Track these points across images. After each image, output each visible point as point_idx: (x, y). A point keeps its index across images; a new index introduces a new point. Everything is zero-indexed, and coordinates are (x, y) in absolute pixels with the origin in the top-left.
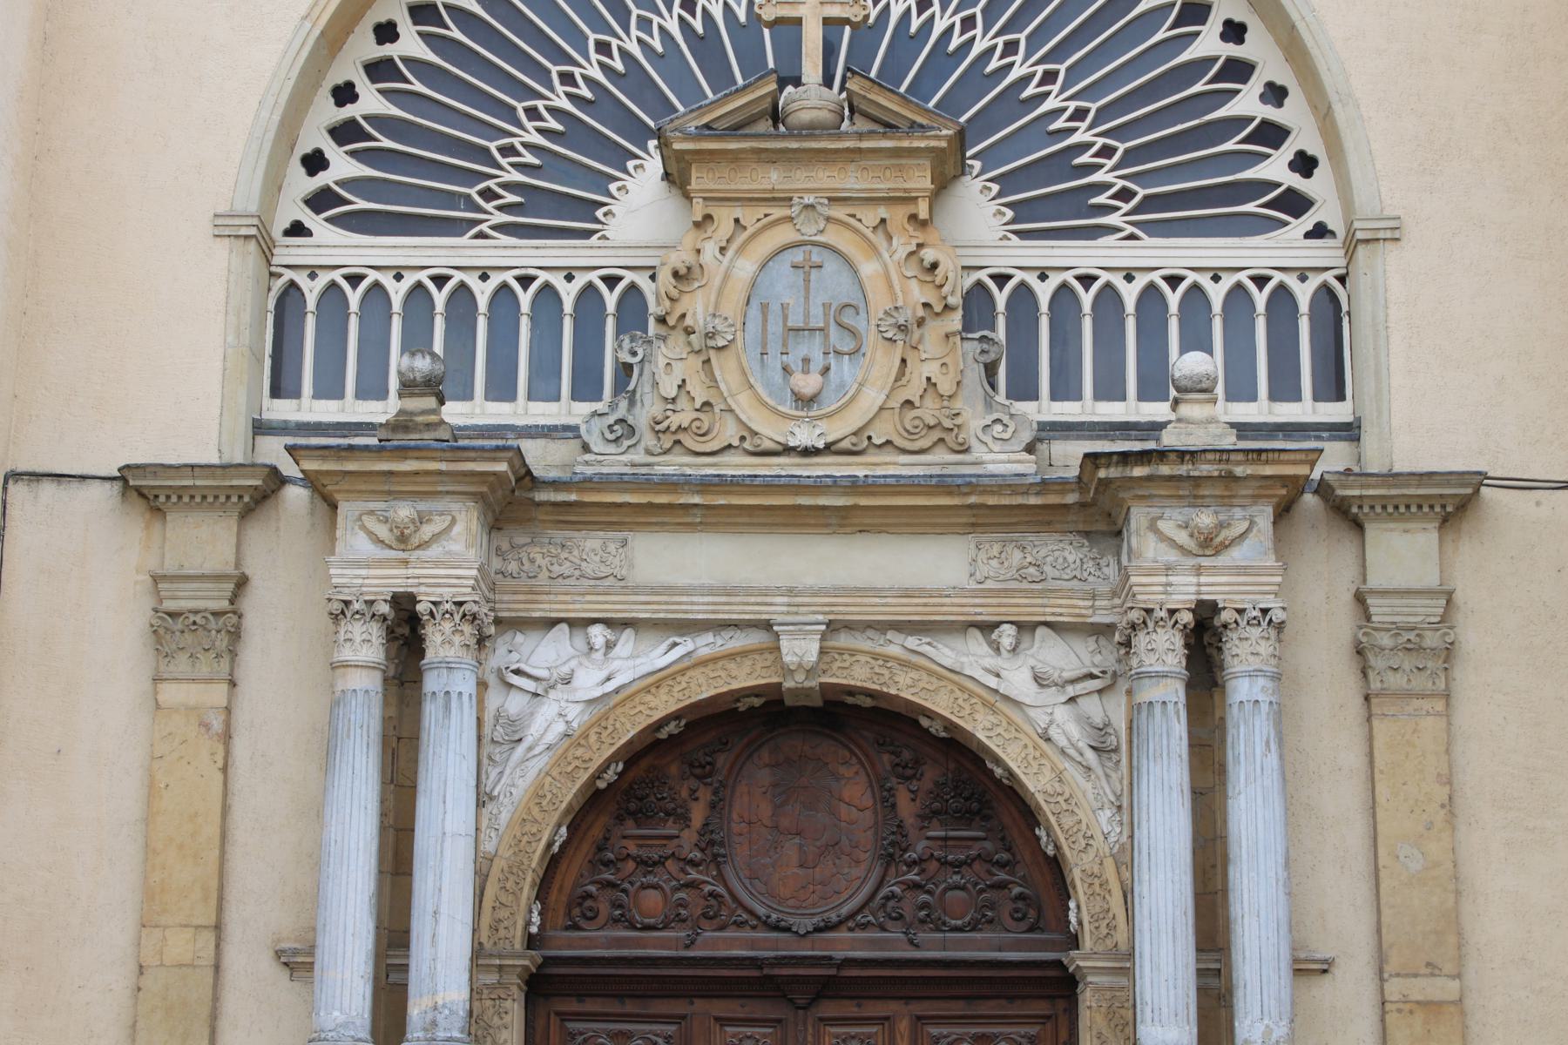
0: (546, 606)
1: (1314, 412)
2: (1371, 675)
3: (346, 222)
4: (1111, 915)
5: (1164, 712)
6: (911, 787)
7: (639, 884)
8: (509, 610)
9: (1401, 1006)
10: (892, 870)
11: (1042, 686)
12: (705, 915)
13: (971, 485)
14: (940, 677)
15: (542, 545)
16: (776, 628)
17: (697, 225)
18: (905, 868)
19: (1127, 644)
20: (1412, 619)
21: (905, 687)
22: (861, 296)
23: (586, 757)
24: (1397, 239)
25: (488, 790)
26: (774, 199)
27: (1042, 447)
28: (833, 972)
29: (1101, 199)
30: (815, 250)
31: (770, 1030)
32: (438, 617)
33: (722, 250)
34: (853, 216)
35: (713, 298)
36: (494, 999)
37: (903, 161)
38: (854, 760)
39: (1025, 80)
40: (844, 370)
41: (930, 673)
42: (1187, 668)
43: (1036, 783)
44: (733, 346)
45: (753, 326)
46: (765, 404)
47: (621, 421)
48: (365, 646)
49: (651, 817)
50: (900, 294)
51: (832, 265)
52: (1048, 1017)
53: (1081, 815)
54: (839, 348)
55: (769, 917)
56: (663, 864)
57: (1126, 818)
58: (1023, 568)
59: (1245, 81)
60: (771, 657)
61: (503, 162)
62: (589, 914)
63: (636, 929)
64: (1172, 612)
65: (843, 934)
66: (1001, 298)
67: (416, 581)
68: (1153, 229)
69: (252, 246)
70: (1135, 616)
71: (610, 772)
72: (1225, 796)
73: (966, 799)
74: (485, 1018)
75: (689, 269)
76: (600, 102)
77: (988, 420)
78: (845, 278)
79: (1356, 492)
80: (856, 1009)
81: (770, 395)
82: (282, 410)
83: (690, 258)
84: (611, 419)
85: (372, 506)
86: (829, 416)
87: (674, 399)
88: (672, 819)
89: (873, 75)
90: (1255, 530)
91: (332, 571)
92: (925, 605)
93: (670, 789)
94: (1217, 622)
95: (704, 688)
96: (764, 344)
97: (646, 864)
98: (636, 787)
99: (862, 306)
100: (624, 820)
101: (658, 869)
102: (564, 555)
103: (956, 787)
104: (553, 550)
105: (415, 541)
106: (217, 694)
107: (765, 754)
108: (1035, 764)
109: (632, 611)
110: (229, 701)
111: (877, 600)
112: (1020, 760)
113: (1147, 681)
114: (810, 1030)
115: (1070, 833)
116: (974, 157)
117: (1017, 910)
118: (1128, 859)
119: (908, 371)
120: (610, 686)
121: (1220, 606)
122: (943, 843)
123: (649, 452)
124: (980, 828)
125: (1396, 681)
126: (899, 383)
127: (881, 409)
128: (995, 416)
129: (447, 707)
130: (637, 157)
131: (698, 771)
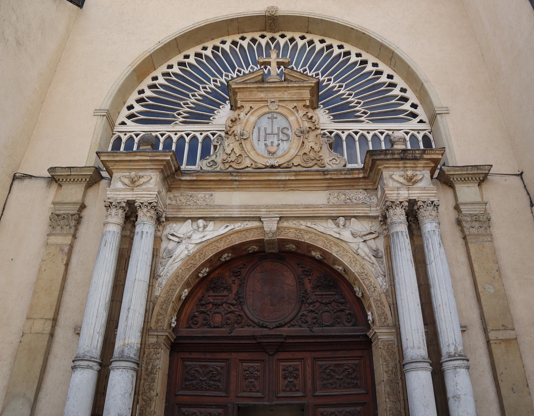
0: (184, 213)
4: (385, 314)
6: (309, 278)
8: (171, 214)
9: (496, 341)
10: (303, 306)
14: (319, 236)
15: (184, 196)
18: (308, 305)
20: (475, 212)
21: (306, 239)
22: (289, 125)
24: (448, 113)
25: (159, 274)
26: (262, 101)
28: (283, 340)
29: (358, 114)
30: (275, 114)
31: (260, 364)
36: (154, 349)
41: (316, 234)
44: (249, 138)
49: (218, 289)
51: (280, 118)
52: (362, 357)
53: (372, 280)
54: (282, 139)
55: (259, 323)
56: (222, 305)
58: (345, 200)
62: (195, 323)
64: (401, 202)
65: (286, 329)
67: (136, 196)
68: (373, 121)
74: (150, 356)
75: (236, 119)
78: (284, 120)
79: (452, 173)
85: (124, 174)
87: (230, 154)
88: (226, 290)
90: (425, 178)
91: (108, 193)
92: (313, 211)
93: (225, 280)
95: (236, 241)
98: (214, 280)
100: (209, 291)
101: (221, 307)
104: (188, 197)
109: (213, 214)
111: (297, 209)
112: (348, 262)
115: (368, 286)
116: (321, 104)
117: (348, 319)
119: (305, 145)
120: (204, 239)
121: (417, 200)
124: (334, 291)
125: (474, 231)
126: (301, 148)
127: (296, 155)
128: (333, 158)
131: (235, 274)
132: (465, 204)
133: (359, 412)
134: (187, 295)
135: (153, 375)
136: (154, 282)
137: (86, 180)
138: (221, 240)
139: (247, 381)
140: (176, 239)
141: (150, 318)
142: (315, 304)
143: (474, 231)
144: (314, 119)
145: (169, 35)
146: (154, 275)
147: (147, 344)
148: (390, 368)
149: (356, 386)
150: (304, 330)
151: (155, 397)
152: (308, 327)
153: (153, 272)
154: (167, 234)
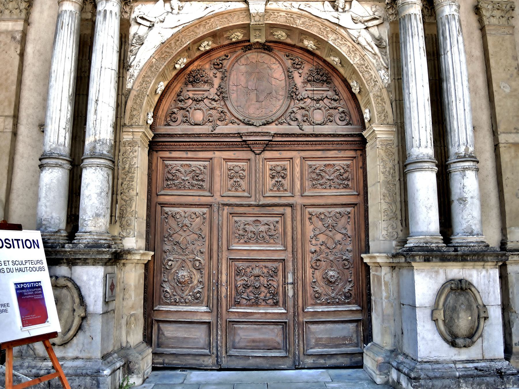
7: (194, 108)
10: (292, 103)
18: (297, 102)
28: (271, 138)
31: (246, 163)
38: (277, 62)
41: (310, 19)
49: (199, 83)
52: (355, 157)
53: (372, 72)
55: (244, 120)
56: (203, 101)
73: (321, 76)
80: (279, 155)
88: (206, 84)
97: (197, 101)
98: (192, 73)
101: (202, 103)
103: (317, 72)
107: (242, 60)
122: (312, 92)
131: (216, 66)
134: (163, 89)
135: (130, 175)
136: (124, 72)
138: (199, 25)
139: (232, 180)
140: (148, 24)
141: (123, 114)
142: (306, 100)
146: (124, 66)
147: (122, 142)
148: (388, 169)
150: (294, 128)
151: (135, 197)
152: (298, 126)
153: (122, 61)
154: (135, 17)
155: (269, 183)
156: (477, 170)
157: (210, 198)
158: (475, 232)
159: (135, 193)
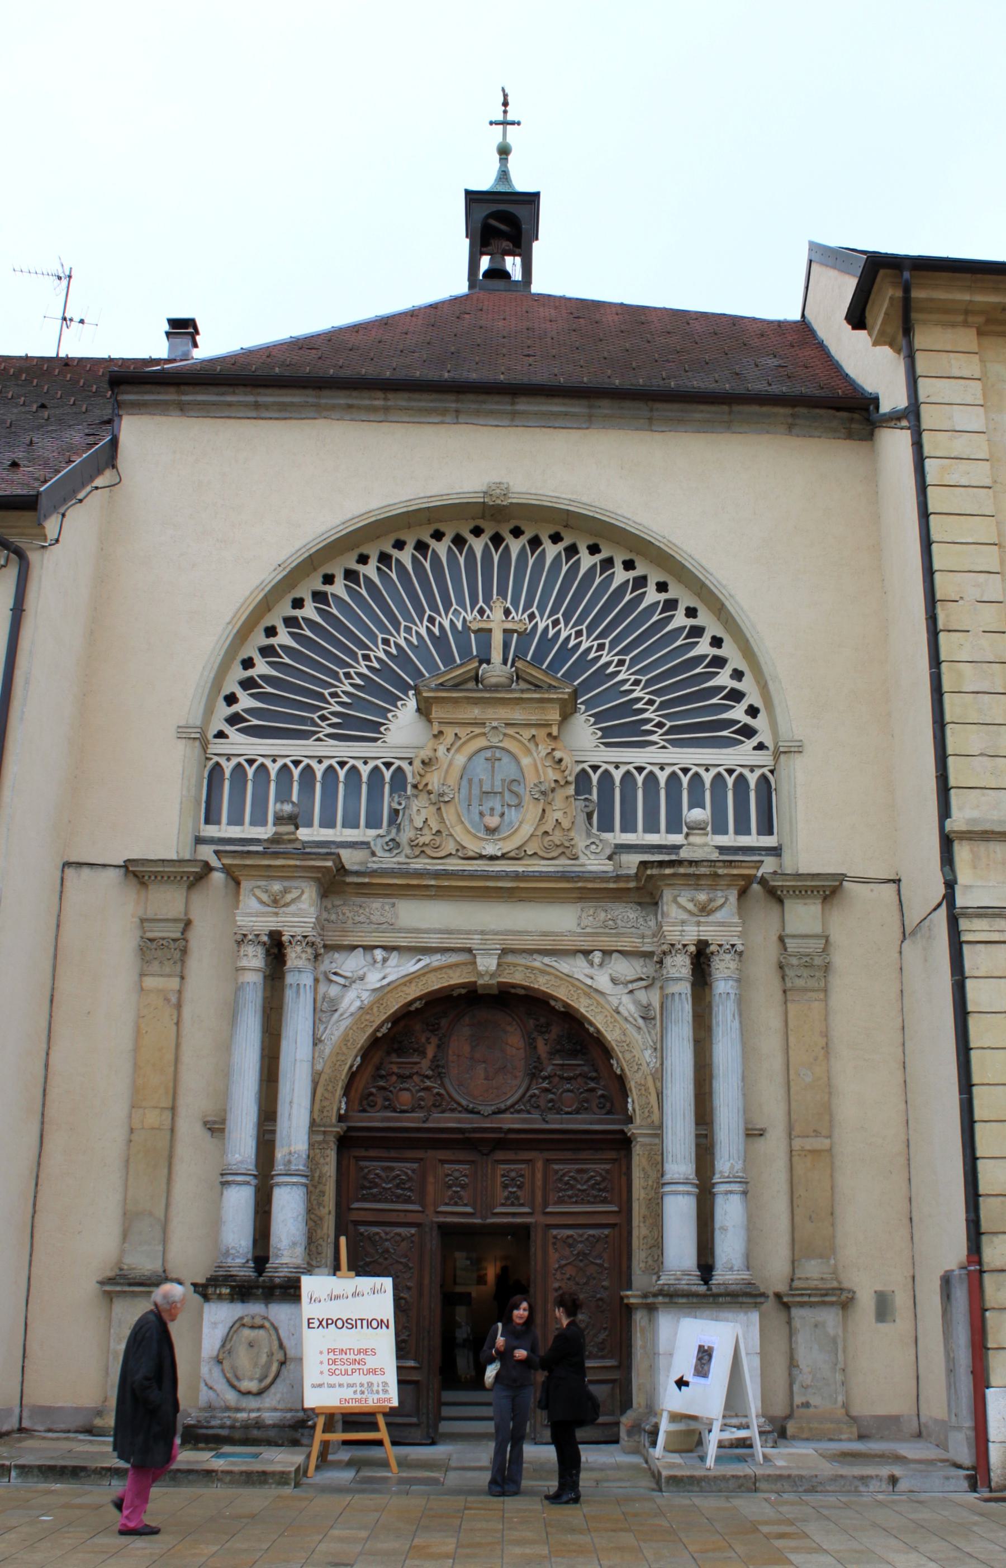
1: (758, 840)
2: (787, 979)
3: (246, 731)
5: (680, 999)
8: (331, 940)
10: (534, 1082)
11: (615, 984)
12: (434, 1105)
13: (579, 877)
14: (561, 979)
16: (474, 952)
17: (435, 736)
18: (541, 1080)
19: (661, 962)
20: (807, 950)
21: (542, 984)
23: (372, 1020)
27: (616, 857)
28: (502, 1135)
29: (648, 727)
30: (498, 751)
32: (294, 943)
33: (448, 750)
34: (518, 733)
35: (443, 775)
37: (545, 705)
38: (514, 1023)
39: (608, 664)
40: (512, 815)
41: (556, 977)
42: (692, 976)
43: (611, 1036)
45: (464, 791)
46: (469, 832)
47: (393, 840)
48: (255, 958)
50: (542, 774)
51: (506, 759)
53: (635, 1053)
54: (510, 803)
57: (659, 1054)
59: (722, 667)
60: (471, 967)
61: (332, 701)
62: (372, 1104)
63: (395, 1111)
64: (685, 946)
65: (508, 1116)
66: (595, 778)
68: (675, 743)
69: (197, 743)
70: (665, 947)
71: (384, 1028)
72: (711, 1044)
73: (574, 1044)
75: (430, 759)
76: (383, 670)
77: (588, 842)
78: (513, 766)
79: (780, 884)
81: (472, 827)
82: (211, 831)
83: (430, 754)
84: (387, 839)
86: (504, 839)
87: (421, 829)
88: (416, 1053)
89: (528, 659)
91: (237, 918)
92: (554, 940)
94: (708, 951)
95: (435, 983)
96: (470, 800)
99: (522, 780)
102: (361, 911)
105: (282, 903)
106: (174, 983)
108: (611, 1026)
110: (181, 987)
111: (528, 937)
113: (671, 982)
114: (490, 1166)
116: (581, 703)
118: (660, 1077)
119: (546, 815)
123: (407, 857)
125: (800, 983)
127: (532, 835)
129: (298, 992)
130: (403, 700)
131: (431, 1028)
132: (794, 936)
133: (607, 1236)
137: (188, 877)
142: (551, 1079)
143: (800, 983)
144: (564, 763)
145: (297, 547)
148: (650, 1183)
149: (604, 1201)
151: (327, 1217)
155: (501, 1194)
156: (745, 1193)
157: (420, 1214)
158: (736, 1268)
159: (326, 1210)
